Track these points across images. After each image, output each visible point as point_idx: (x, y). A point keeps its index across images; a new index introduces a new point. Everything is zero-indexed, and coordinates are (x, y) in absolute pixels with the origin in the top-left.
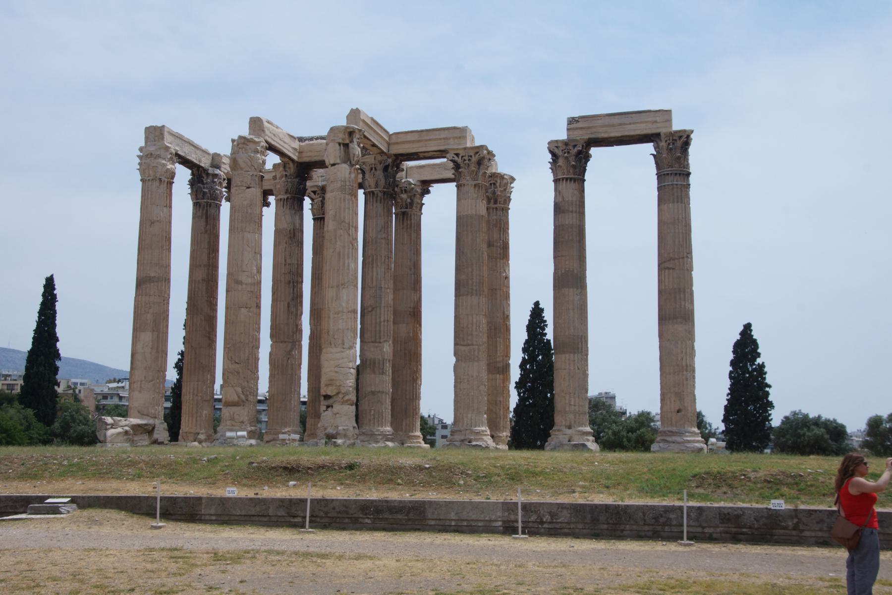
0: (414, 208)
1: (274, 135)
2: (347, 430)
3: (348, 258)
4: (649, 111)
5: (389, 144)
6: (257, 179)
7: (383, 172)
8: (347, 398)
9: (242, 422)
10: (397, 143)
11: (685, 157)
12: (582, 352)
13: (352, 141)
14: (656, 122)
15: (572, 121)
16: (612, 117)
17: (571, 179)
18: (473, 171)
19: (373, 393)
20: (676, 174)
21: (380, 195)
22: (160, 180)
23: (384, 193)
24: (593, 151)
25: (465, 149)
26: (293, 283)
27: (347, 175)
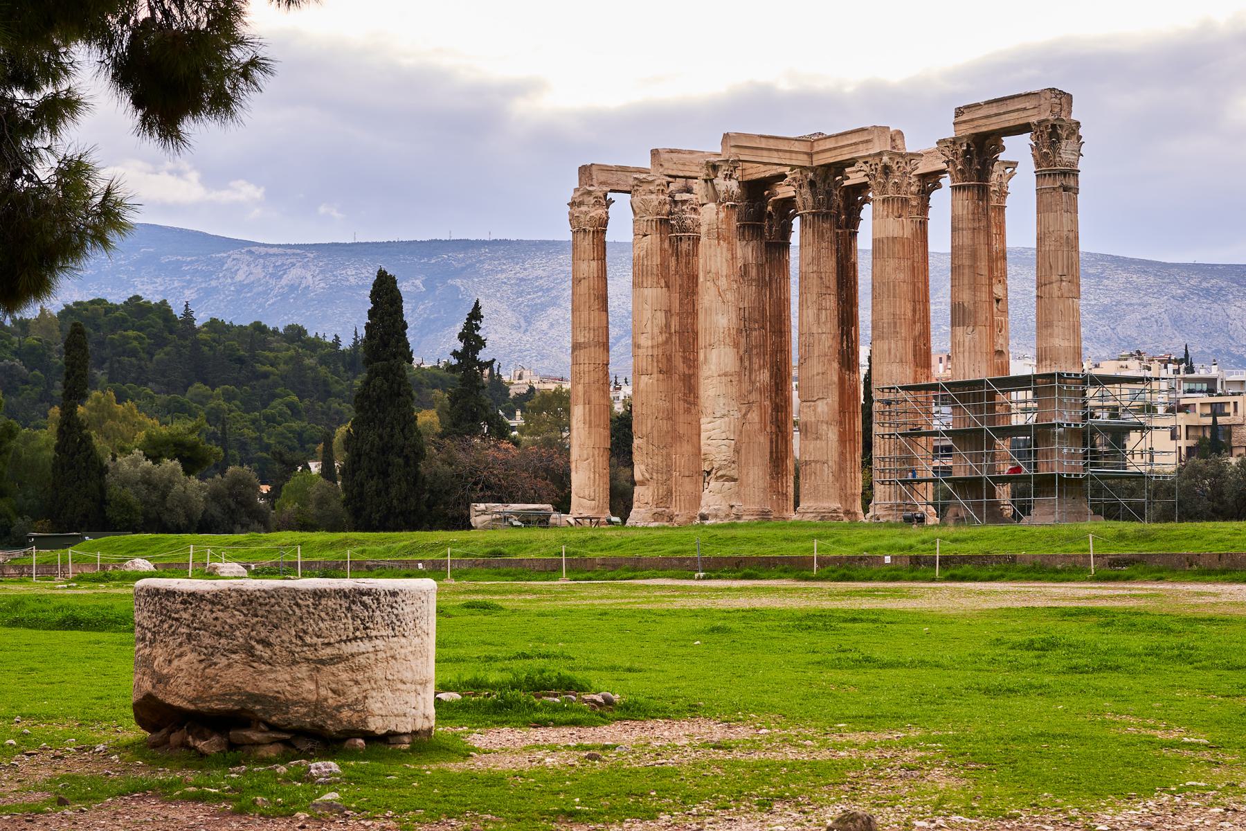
1: (684, 164)
2: (719, 510)
3: (717, 314)
5: (810, 155)
6: (654, 224)
7: (811, 189)
8: (720, 473)
10: (817, 153)
13: (716, 177)
14: (1025, 109)
15: (959, 112)
16: (990, 105)
17: (960, 187)
20: (1045, 175)
22: (584, 230)
24: (1006, 141)
25: (869, 156)
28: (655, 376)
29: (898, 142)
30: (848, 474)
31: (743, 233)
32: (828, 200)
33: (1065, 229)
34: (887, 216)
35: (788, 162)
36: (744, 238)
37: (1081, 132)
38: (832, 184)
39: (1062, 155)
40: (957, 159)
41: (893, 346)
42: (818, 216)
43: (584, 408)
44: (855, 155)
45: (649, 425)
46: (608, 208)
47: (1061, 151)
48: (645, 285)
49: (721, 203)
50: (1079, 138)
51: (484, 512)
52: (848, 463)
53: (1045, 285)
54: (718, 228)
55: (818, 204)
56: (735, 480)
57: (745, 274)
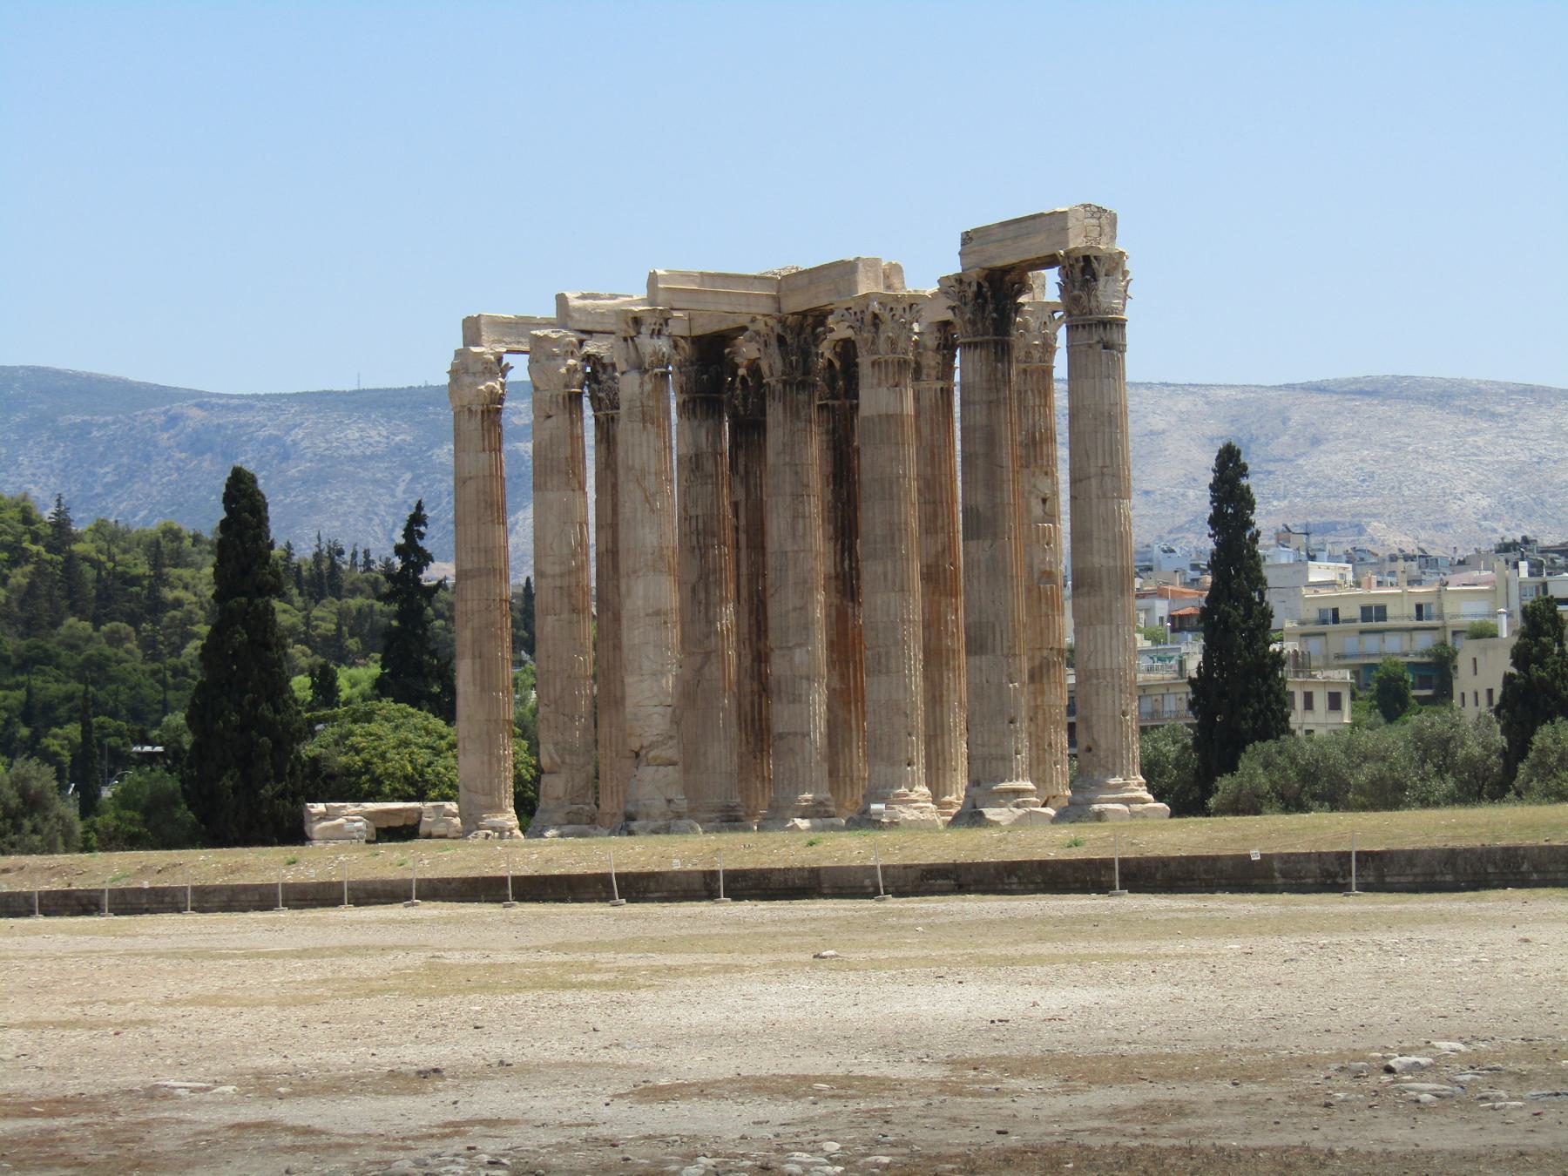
0: (924, 377)
3: (643, 527)
4: (1042, 215)
6: (560, 400)
7: (780, 346)
8: (652, 754)
9: (558, 798)
11: (1089, 294)
12: (994, 651)
13: (639, 333)
15: (967, 238)
18: (866, 339)
19: (781, 736)
20: (1077, 326)
21: (780, 386)
22: (470, 410)
23: (785, 383)
26: (700, 549)
27: (637, 389)
28: (565, 616)
29: (896, 282)
30: (854, 750)
31: (694, 409)
32: (805, 361)
33: (1106, 402)
34: (879, 385)
35: (744, 310)
36: (696, 417)
37: (1128, 265)
38: (810, 339)
39: (1101, 298)
40: (966, 304)
41: (890, 567)
42: (791, 385)
43: (474, 664)
44: (834, 299)
45: (558, 687)
46: (504, 376)
47: (1099, 293)
48: (549, 485)
49: (646, 371)
50: (1125, 273)
51: (324, 817)
52: (854, 733)
53: (1081, 480)
54: (642, 406)
55: (789, 367)
56: (674, 764)
57: (697, 467)
